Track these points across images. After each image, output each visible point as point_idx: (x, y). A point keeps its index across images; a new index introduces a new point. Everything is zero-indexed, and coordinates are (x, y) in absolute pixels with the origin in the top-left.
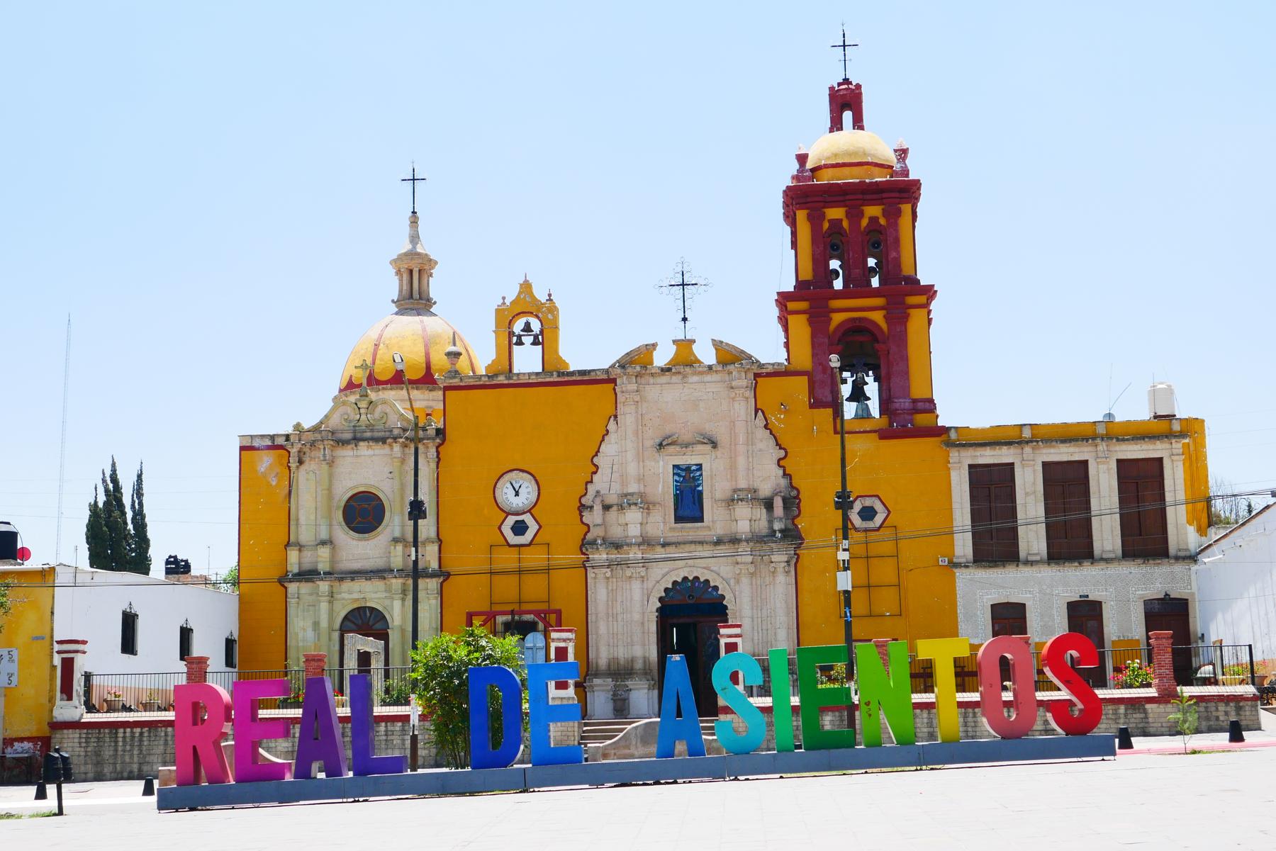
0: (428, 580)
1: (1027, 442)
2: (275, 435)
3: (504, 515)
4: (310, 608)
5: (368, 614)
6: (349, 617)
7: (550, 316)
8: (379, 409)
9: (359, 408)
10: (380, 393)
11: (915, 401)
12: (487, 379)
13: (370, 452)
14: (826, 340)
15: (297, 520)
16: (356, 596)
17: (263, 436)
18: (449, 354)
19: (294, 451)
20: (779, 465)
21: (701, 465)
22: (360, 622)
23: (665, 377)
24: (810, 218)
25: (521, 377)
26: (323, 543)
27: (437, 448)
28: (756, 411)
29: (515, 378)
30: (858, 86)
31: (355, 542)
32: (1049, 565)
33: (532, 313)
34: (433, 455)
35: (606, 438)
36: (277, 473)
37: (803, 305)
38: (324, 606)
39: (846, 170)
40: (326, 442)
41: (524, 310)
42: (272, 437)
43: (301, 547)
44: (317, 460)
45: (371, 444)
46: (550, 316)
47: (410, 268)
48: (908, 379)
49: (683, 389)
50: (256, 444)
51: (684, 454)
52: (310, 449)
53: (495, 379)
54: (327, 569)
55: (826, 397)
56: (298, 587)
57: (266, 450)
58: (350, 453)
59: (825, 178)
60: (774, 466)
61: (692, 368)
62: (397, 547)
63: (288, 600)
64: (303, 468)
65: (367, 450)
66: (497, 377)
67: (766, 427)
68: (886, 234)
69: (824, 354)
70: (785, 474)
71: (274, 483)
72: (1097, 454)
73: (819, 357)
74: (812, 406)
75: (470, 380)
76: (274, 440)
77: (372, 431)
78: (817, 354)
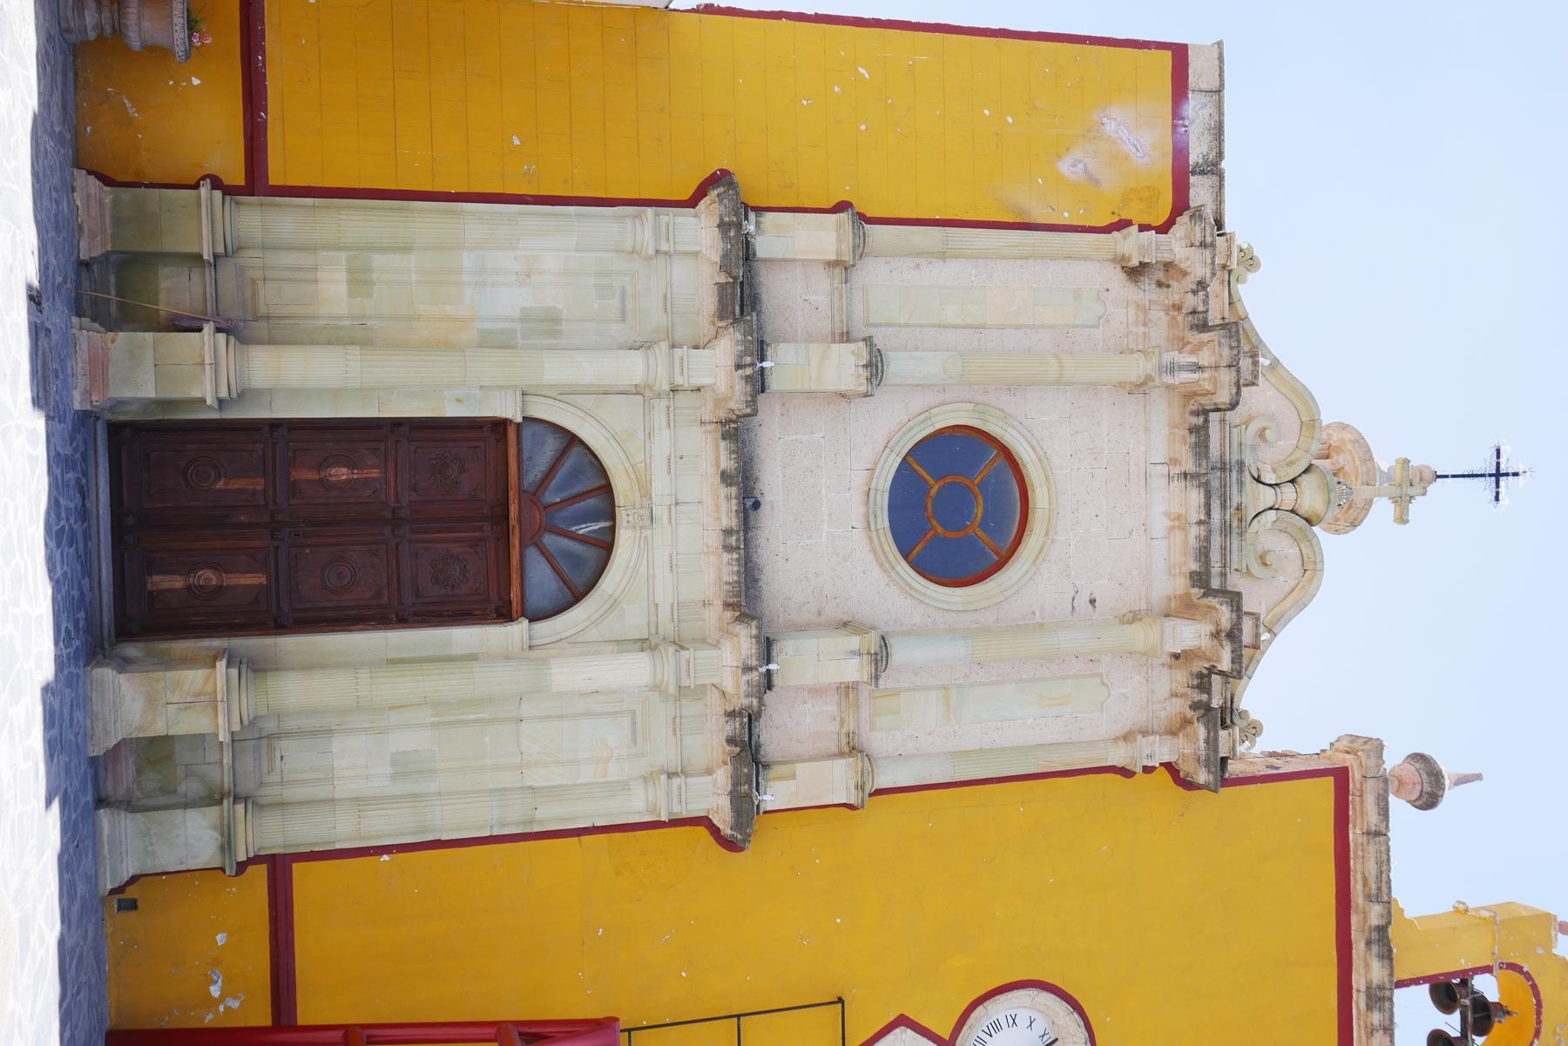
0: (722, 777)
2: (1220, 176)
3: (946, 1035)
4: (615, 303)
5: (584, 529)
6: (576, 450)
8: (1283, 548)
9: (1293, 481)
13: (1160, 524)
15: (942, 256)
16: (661, 486)
17: (1218, 132)
22: (551, 497)
26: (875, 367)
27: (1169, 767)
29: (1376, 1017)
31: (859, 479)
34: (1150, 757)
36: (1093, 180)
38: (631, 369)
40: (1226, 377)
41: (1544, 1010)
42: (1213, 168)
43: (842, 267)
44: (1142, 329)
45: (1194, 531)
50: (1196, 107)
52: (1177, 308)
53: (1375, 949)
54: (774, 383)
56: (696, 254)
57: (1175, 143)
58: (1160, 452)
62: (854, 662)
63: (650, 211)
65: (1168, 515)
66: (1381, 957)
71: (1065, 167)
75: (1372, 867)
76: (1203, 173)
77: (1226, 530)
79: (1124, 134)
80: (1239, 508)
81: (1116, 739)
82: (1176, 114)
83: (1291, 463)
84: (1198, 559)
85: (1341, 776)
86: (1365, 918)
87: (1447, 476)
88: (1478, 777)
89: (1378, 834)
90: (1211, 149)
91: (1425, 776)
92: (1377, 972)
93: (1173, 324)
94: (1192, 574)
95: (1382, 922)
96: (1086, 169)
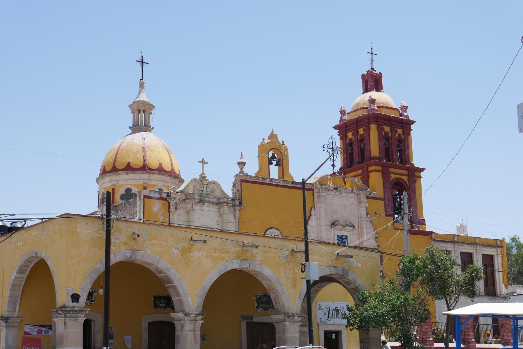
1: (458, 242)
7: (286, 153)
8: (211, 186)
9: (203, 184)
10: (152, 175)
12: (262, 180)
13: (208, 209)
18: (239, 163)
19: (172, 203)
21: (347, 236)
23: (333, 192)
24: (378, 129)
25: (276, 181)
29: (274, 181)
30: (380, 73)
32: (465, 296)
33: (278, 150)
35: (311, 217)
36: (163, 214)
37: (380, 168)
39: (390, 110)
41: (275, 148)
44: (183, 209)
46: (286, 153)
47: (139, 109)
49: (340, 199)
50: (152, 195)
51: (341, 230)
59: (384, 112)
60: (374, 240)
61: (346, 190)
64: (177, 212)
65: (207, 207)
66: (266, 179)
68: (404, 142)
72: (477, 251)
76: (161, 195)
79: (156, 208)
80: (206, 195)
81: (235, 220)
82: (153, 198)
83: (200, 184)
84: (214, 205)
85: (242, 181)
86: (261, 180)
87: (142, 77)
88: (242, 152)
89: (251, 177)
90: (158, 193)
91: (242, 164)
92: (268, 180)
93: (182, 203)
94: (216, 205)
95: (262, 178)
96: (161, 215)
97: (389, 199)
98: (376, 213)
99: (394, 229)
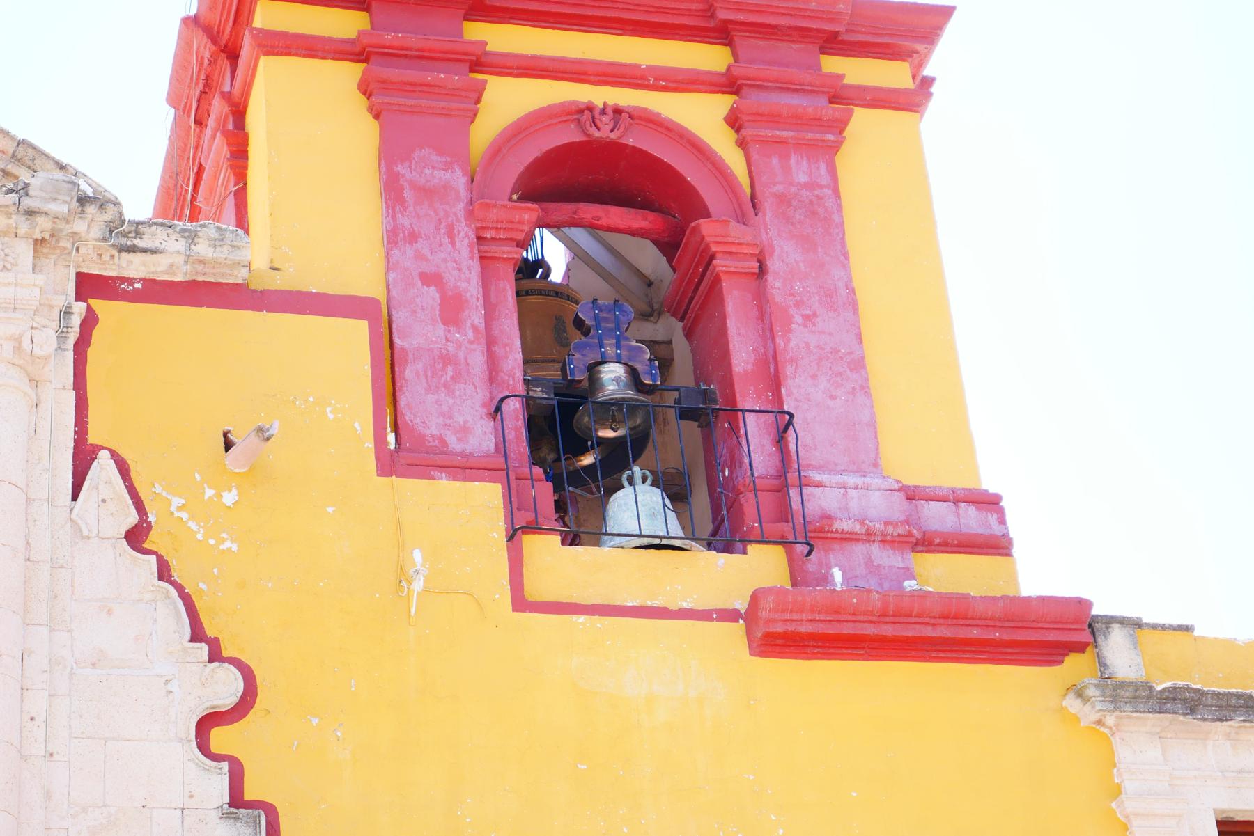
11: (913, 495)
14: (459, 181)
20: (204, 747)
28: (83, 458)
48: (865, 388)
55: (464, 431)
67: (136, 537)
69: (451, 234)
70: (237, 800)
73: (421, 245)
74: (389, 464)
78: (413, 237)
97: (451, 310)
98: (228, 445)
99: (521, 603)
